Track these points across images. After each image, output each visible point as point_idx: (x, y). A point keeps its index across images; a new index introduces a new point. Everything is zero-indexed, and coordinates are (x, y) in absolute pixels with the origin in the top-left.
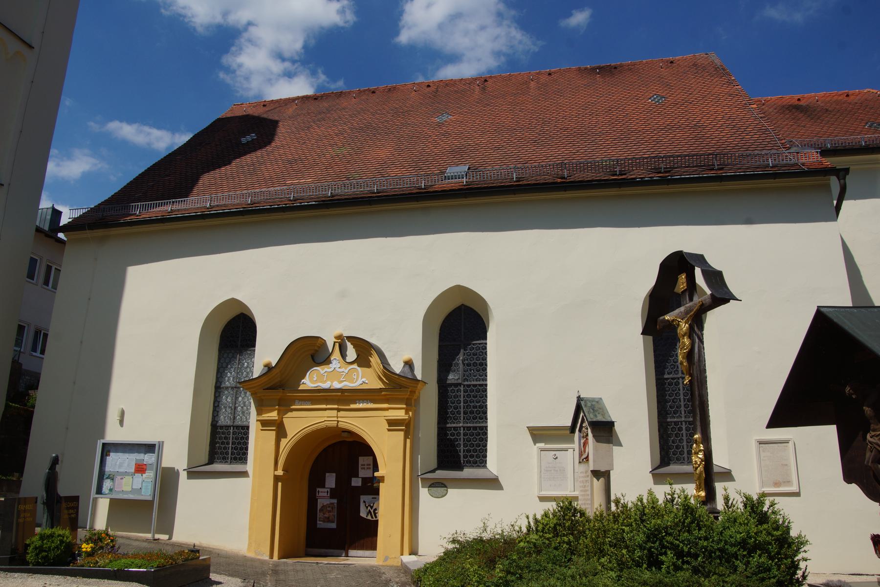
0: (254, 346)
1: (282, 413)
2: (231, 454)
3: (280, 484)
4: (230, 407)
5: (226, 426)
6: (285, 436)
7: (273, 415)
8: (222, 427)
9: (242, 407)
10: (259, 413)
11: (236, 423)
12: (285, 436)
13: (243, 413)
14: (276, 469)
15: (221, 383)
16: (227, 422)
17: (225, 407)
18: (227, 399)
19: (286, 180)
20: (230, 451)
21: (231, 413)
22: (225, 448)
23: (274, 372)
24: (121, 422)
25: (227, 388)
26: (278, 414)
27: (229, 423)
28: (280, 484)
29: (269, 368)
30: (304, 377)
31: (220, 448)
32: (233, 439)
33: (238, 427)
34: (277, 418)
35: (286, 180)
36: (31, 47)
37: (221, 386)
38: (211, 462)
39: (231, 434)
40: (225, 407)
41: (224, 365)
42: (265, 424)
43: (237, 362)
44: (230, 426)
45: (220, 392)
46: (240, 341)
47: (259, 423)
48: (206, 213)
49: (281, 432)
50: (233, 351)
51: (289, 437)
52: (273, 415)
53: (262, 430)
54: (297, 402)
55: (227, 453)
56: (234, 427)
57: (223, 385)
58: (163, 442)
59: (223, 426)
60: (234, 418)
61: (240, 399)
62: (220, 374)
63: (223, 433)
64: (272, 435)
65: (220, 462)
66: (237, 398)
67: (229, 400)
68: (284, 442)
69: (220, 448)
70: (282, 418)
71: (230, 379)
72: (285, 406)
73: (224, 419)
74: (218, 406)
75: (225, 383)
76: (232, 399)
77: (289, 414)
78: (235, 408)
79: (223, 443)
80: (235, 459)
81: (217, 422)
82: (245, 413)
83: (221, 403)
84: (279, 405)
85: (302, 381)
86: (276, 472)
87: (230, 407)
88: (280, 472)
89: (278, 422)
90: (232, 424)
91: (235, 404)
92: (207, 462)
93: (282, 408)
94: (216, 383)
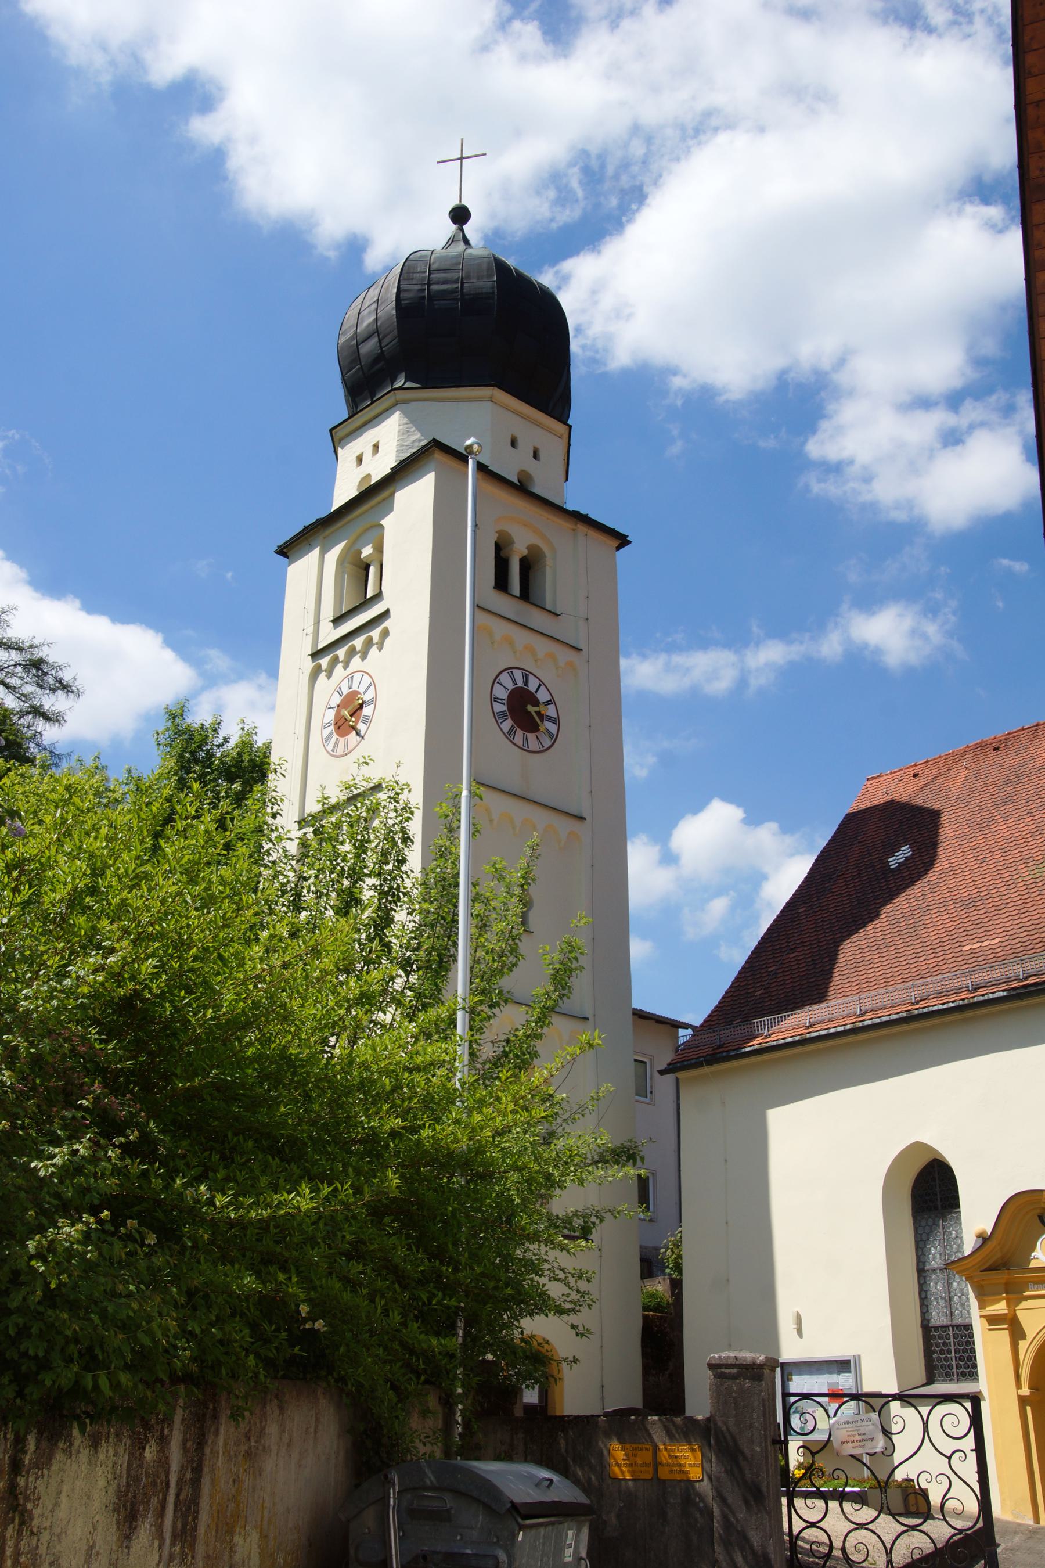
0: (959, 1206)
1: (1012, 1304)
2: (957, 1368)
3: (1029, 1409)
4: (943, 1298)
5: (943, 1327)
6: (1023, 1337)
7: (1000, 1307)
8: (936, 1328)
9: (960, 1297)
10: (982, 1306)
11: (955, 1322)
12: (1023, 1337)
13: (963, 1305)
14: (1019, 1385)
15: (924, 1263)
16: (943, 1320)
17: (936, 1299)
18: (936, 1287)
20: (954, 1363)
21: (946, 1307)
22: (946, 1359)
23: (990, 1245)
24: (799, 1332)
25: (934, 1270)
26: (1008, 1305)
27: (946, 1321)
28: (1029, 1409)
29: (984, 1239)
30: (1033, 1248)
31: (939, 1359)
32: (955, 1345)
33: (958, 1326)
34: (1006, 1312)
36: (582, 818)
37: (926, 1269)
38: (930, 1381)
39: (952, 1337)
40: (936, 1299)
41: (924, 1237)
42: (993, 1320)
43: (941, 1230)
44: (948, 1327)
45: (925, 1277)
46: (939, 1200)
47: (984, 1320)
49: (1017, 1333)
50: (933, 1216)
51: (1029, 1338)
52: (1000, 1307)
53: (990, 1330)
54: (1031, 1285)
55: (950, 1367)
56: (953, 1327)
57: (927, 1267)
58: (859, 1356)
59: (938, 1327)
60: (952, 1314)
61: (955, 1284)
62: (920, 1250)
63: (940, 1337)
64: (1004, 1336)
65: (943, 1381)
66: (950, 1284)
67: (940, 1287)
68: (1023, 1345)
69: (939, 1359)
70: (1015, 1310)
71: (935, 1259)
72: (1015, 1292)
73: (938, 1317)
74: (926, 1297)
75: (930, 1264)
76: (944, 1286)
77: (1024, 1305)
78: (950, 1299)
79: (942, 1352)
80: (963, 1374)
81: (929, 1321)
82: (965, 1305)
83: (929, 1293)
84: (1007, 1293)
85: (1033, 1255)
86: (1019, 1391)
87: (943, 1298)
88: (1025, 1391)
89: (1010, 1316)
90: (949, 1323)
91: (949, 1293)
92: (925, 1381)
93: (1011, 1296)
94: (918, 1265)
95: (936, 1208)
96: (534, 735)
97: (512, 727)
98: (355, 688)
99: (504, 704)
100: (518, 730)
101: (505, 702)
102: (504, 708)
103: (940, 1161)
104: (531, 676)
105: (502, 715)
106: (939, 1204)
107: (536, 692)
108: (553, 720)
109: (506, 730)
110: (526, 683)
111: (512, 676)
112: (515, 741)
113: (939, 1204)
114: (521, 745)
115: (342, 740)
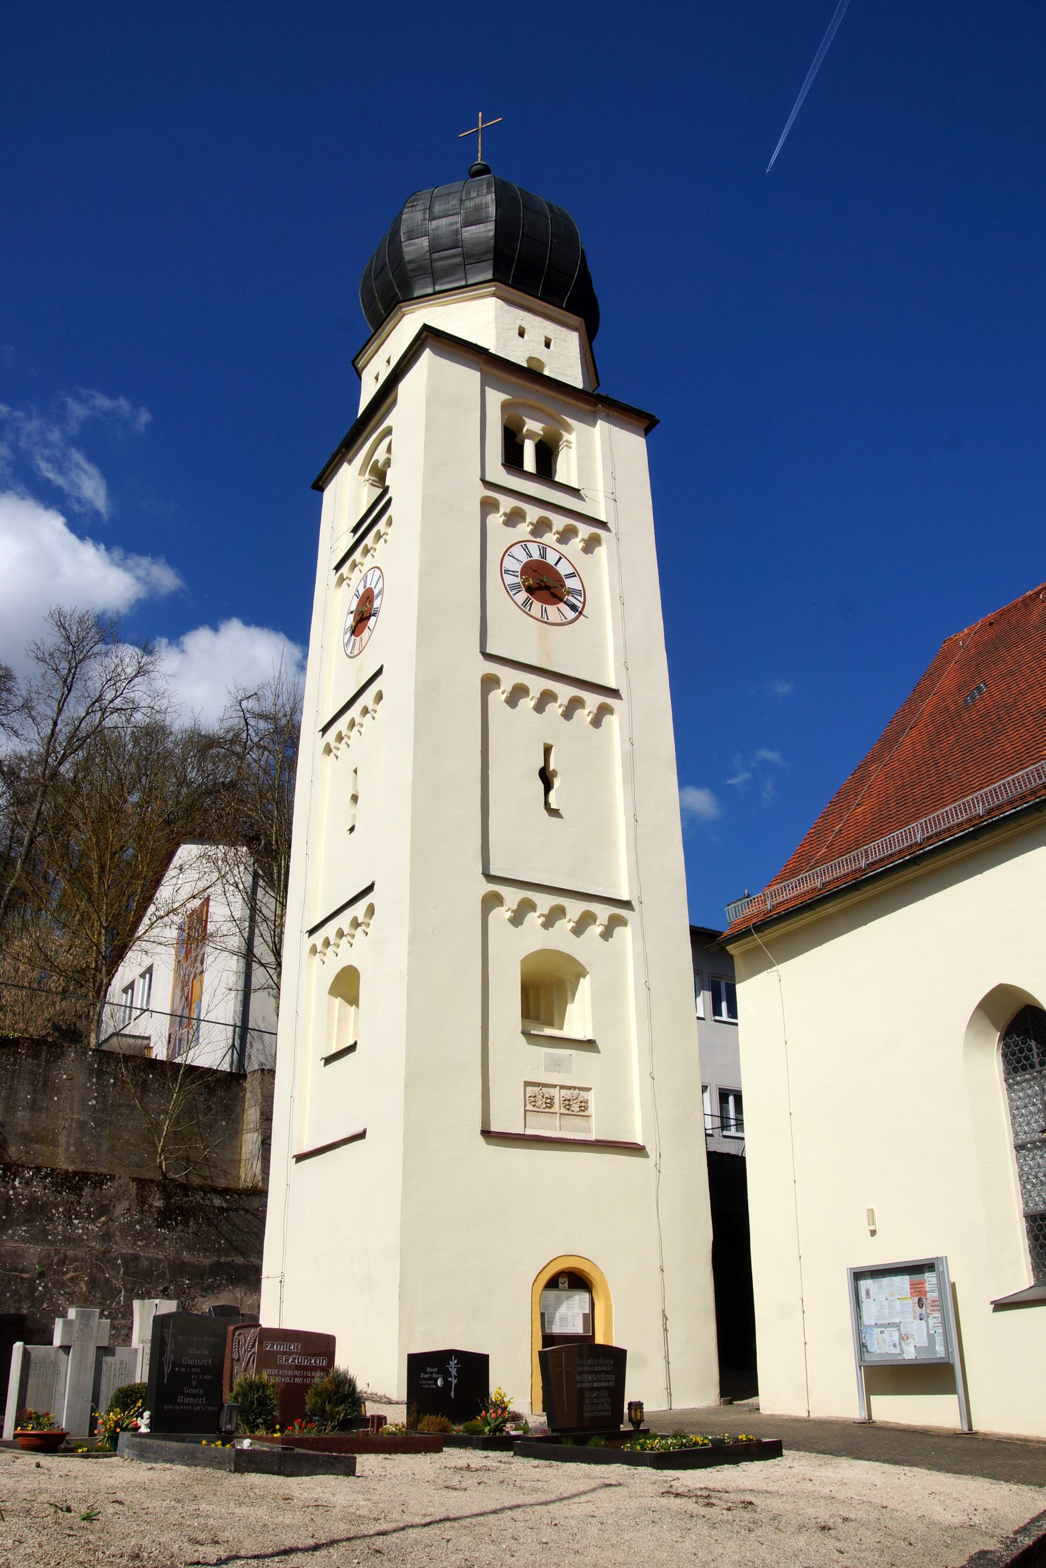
19: (1040, 749)
35: (1040, 749)
48: (918, 853)
58: (946, 1257)
95: (1032, 1066)
96: (555, 607)
97: (527, 600)
98: (368, 586)
99: (517, 576)
100: (535, 602)
101: (519, 574)
102: (518, 580)
103: (1039, 1009)
104: (548, 549)
105: (515, 587)
106: (1036, 1060)
107: (556, 565)
108: (579, 592)
109: (520, 603)
110: (543, 555)
111: (526, 549)
112: (532, 613)
113: (1036, 1060)
114: (539, 617)
115: (358, 639)
